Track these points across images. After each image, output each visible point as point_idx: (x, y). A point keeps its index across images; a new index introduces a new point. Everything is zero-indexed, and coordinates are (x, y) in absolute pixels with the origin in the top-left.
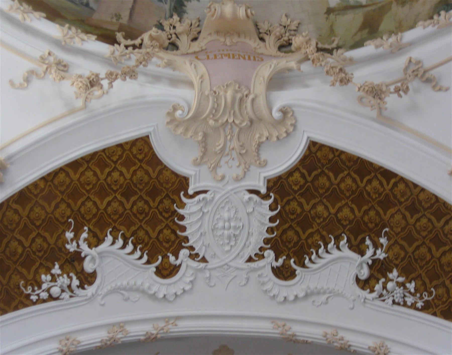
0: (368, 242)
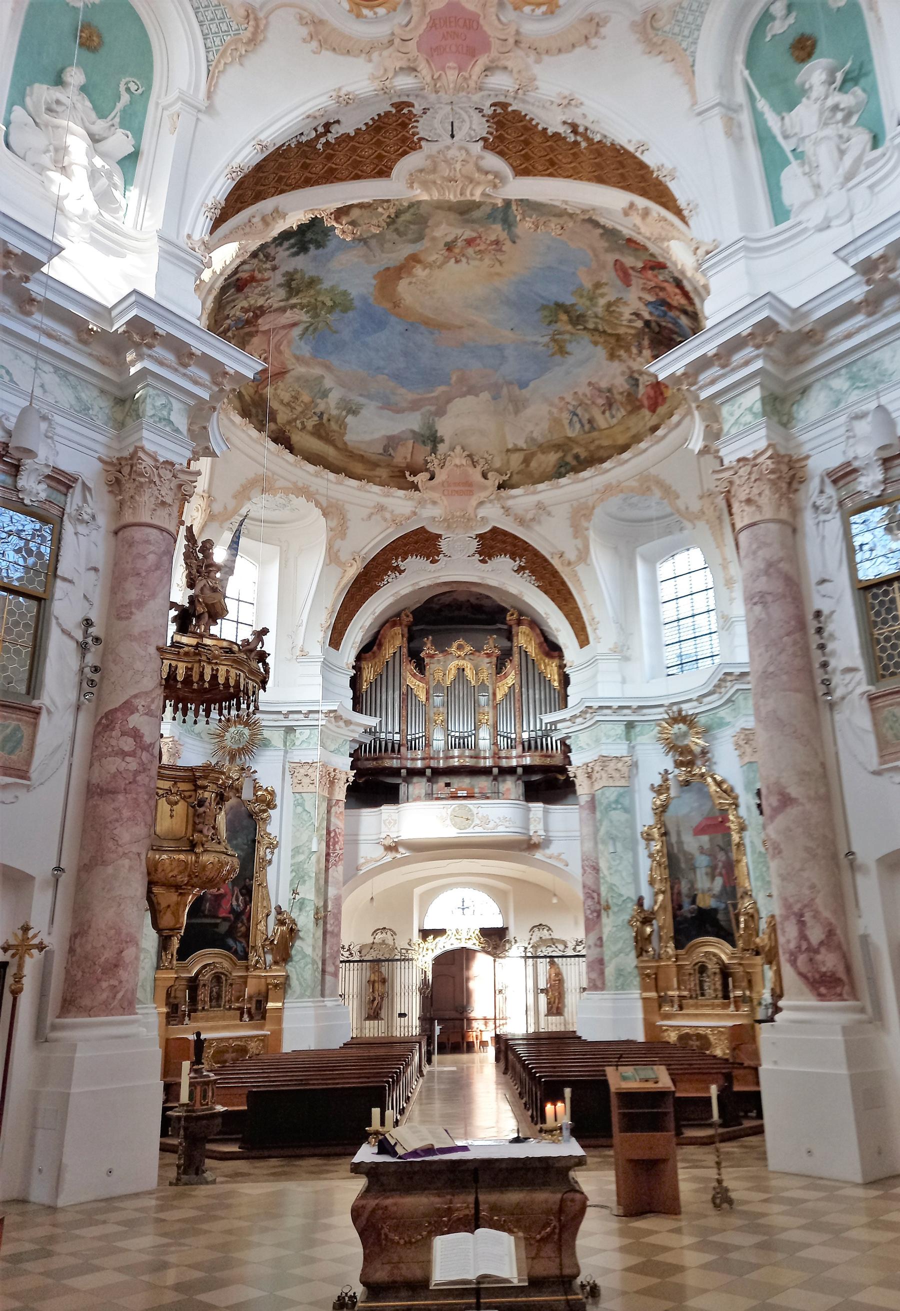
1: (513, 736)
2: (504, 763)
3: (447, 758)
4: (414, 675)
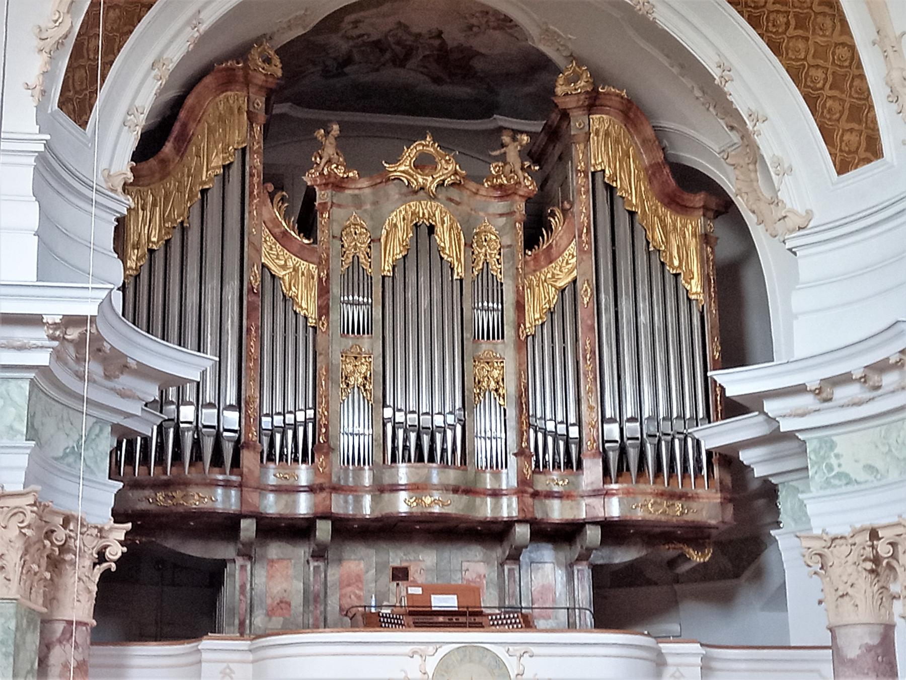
1: (574, 432)
4: (283, 238)
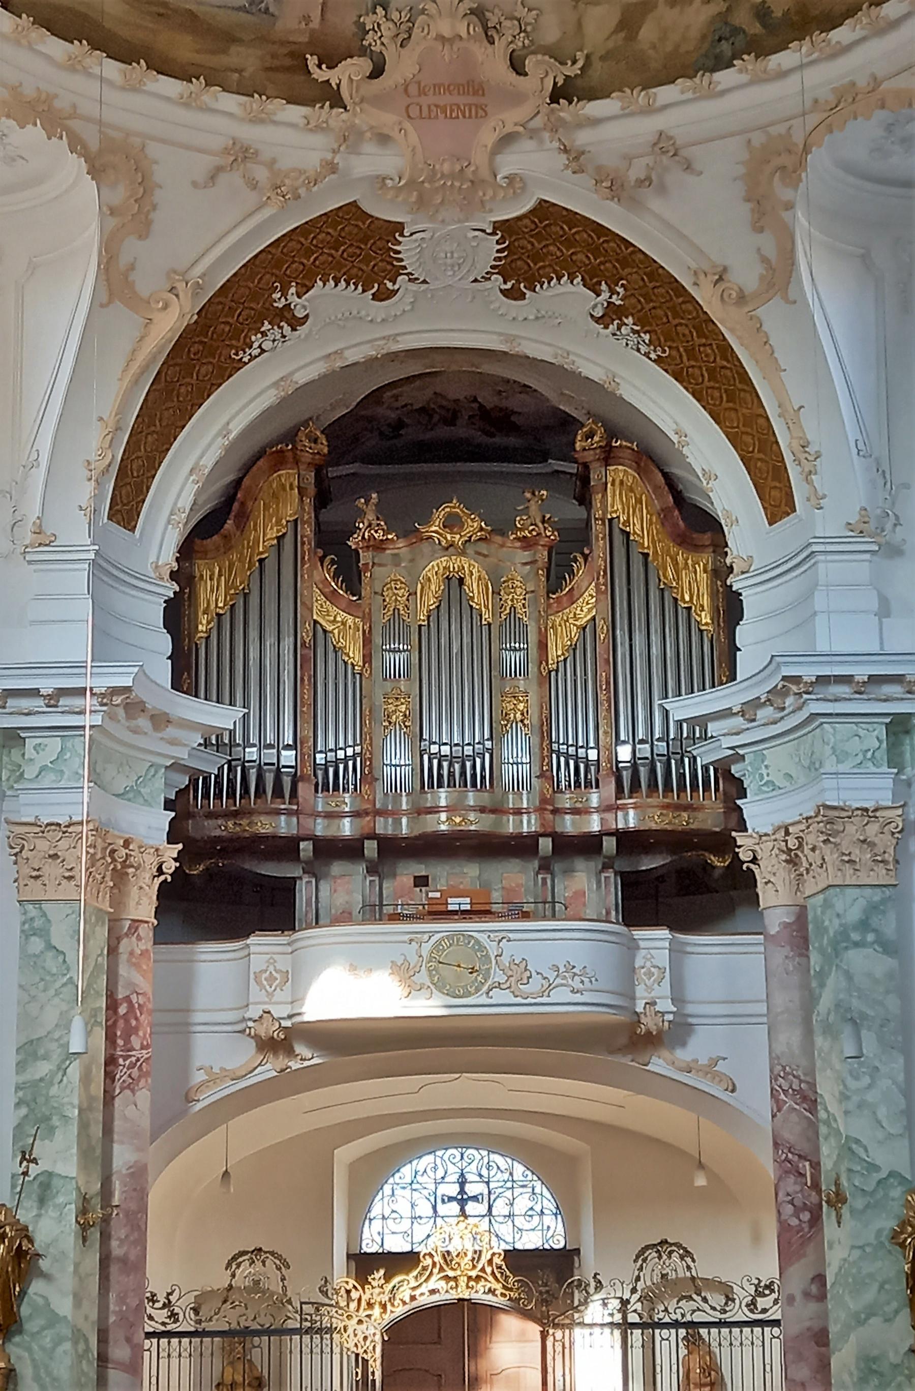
0: (604, 287)
1: (593, 755)
2: (568, 825)
3: (420, 811)
4: (332, 597)
